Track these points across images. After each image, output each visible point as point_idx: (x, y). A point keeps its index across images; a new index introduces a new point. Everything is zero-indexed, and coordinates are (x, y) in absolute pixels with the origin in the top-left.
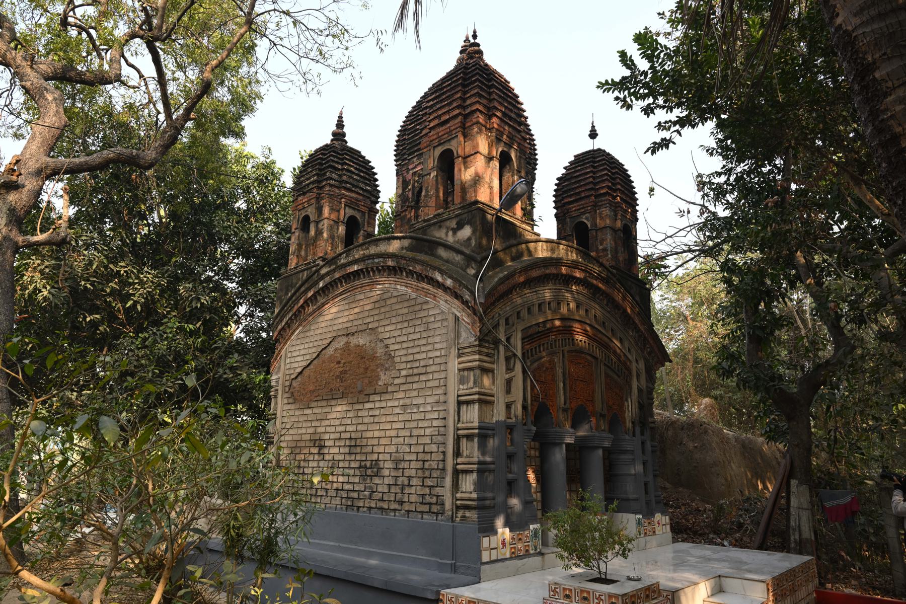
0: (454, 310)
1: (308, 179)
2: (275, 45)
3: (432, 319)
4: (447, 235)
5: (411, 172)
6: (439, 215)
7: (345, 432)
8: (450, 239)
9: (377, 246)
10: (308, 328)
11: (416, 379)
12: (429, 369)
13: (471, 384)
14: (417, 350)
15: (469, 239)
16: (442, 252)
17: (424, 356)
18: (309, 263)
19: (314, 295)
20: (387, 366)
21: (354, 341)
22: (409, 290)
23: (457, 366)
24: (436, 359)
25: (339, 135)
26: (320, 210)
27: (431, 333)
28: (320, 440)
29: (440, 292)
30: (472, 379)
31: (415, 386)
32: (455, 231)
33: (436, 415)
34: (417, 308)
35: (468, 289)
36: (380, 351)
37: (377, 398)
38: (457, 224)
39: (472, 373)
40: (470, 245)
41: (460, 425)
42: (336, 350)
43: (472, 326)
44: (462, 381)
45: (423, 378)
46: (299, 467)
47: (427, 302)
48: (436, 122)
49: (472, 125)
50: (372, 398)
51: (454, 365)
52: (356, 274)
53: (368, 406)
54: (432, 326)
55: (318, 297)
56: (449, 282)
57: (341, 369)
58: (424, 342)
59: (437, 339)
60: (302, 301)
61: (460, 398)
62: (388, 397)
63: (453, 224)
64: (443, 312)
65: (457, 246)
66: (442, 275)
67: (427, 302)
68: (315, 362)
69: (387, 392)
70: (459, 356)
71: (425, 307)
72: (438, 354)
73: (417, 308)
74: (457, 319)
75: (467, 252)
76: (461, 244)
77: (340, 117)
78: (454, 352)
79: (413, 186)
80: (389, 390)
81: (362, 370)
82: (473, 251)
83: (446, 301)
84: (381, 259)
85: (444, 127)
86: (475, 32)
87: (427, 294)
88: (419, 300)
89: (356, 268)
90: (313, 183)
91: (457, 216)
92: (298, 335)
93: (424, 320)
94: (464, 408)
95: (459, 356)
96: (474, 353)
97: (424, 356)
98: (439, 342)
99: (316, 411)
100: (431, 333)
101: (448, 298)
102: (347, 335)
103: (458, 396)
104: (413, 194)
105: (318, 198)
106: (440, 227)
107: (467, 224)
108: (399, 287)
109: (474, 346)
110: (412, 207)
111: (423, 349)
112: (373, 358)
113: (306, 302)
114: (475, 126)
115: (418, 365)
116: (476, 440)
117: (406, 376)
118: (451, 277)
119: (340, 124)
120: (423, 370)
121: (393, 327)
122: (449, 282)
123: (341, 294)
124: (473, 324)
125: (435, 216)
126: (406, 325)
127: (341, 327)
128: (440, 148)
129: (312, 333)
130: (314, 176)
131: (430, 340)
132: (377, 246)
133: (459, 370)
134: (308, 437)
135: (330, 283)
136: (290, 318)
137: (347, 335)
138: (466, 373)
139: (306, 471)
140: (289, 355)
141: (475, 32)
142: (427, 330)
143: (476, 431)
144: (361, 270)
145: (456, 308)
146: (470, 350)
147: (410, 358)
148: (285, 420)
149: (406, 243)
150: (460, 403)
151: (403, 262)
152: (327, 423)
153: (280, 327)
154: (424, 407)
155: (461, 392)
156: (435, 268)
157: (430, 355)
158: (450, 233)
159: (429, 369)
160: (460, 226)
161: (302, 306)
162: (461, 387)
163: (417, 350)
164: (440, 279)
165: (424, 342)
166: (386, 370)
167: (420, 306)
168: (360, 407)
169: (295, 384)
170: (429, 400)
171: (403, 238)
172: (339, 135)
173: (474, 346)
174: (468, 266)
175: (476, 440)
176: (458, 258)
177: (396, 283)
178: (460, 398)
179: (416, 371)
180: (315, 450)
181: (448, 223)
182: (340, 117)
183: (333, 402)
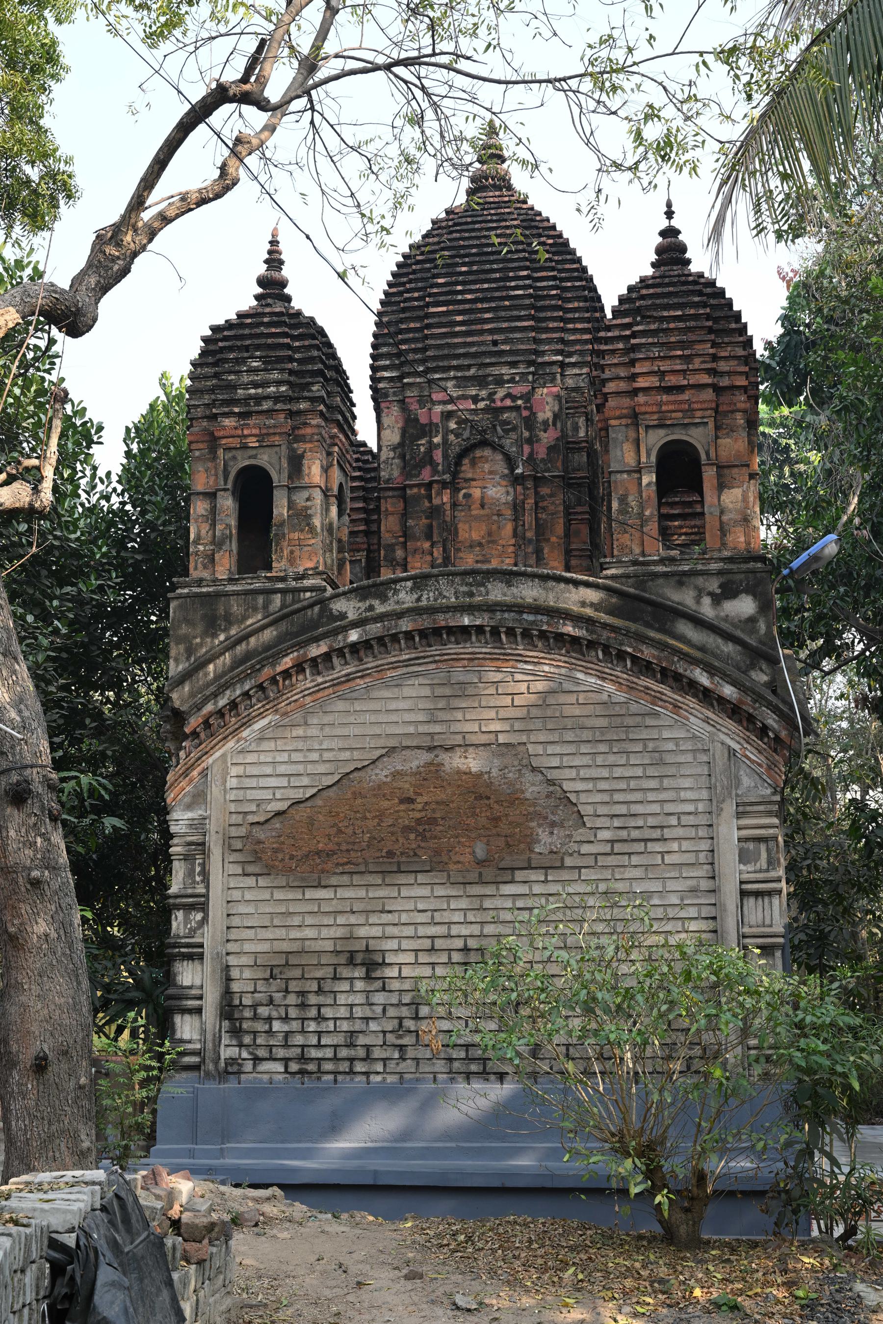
0: (723, 737)
1: (256, 385)
2: (312, 109)
3: (671, 746)
4: (698, 602)
5: (438, 409)
6: (672, 560)
7: (449, 936)
8: (707, 609)
9: (509, 584)
10: (297, 717)
11: (640, 847)
12: (668, 833)
13: (763, 863)
14: (638, 796)
15: (752, 620)
16: (685, 628)
17: (656, 808)
18: (283, 579)
19: (327, 657)
20: (556, 818)
21: (456, 762)
22: (610, 687)
23: (736, 834)
24: (683, 817)
25: (272, 286)
26: (296, 464)
27: (671, 771)
28: (367, 950)
29: (691, 702)
30: (764, 855)
31: (635, 860)
32: (717, 600)
33: (693, 912)
34: (629, 721)
35: (776, 710)
36: (532, 787)
37: (535, 875)
38: (720, 587)
39: (763, 847)
40: (754, 631)
41: (746, 930)
42: (396, 774)
43: (769, 767)
44: (744, 857)
45: (652, 847)
46: (303, 1006)
47: (656, 715)
48: (654, 381)
49: (733, 412)
50: (519, 875)
51: (729, 832)
52: (465, 630)
53: (507, 889)
54: (669, 758)
55: (335, 660)
56: (728, 691)
57: (418, 815)
58: (653, 784)
59: (687, 783)
60: (287, 662)
61: (744, 886)
62: (565, 875)
63: (714, 585)
64: (695, 737)
65: (724, 626)
66: (712, 675)
67: (656, 715)
68: (331, 793)
69: (562, 867)
70: (739, 815)
71: (649, 721)
72: (690, 808)
73: (629, 721)
74: (731, 753)
75: (752, 641)
76: (733, 625)
77: (274, 243)
78: (730, 808)
79: (445, 440)
80: (568, 862)
81: (483, 821)
82: (761, 642)
83: (706, 720)
84: (545, 618)
85: (672, 398)
86: (669, 205)
87: (656, 699)
88: (634, 708)
89: (466, 621)
90: (277, 398)
91: (720, 573)
92: (262, 730)
93: (651, 745)
94: (751, 902)
95: (739, 815)
96: (769, 814)
97: (656, 808)
98: (689, 791)
99: (342, 893)
100: (671, 771)
101: (710, 714)
102: (430, 749)
103: (741, 883)
104: (445, 456)
105: (293, 436)
106: (681, 584)
107: (747, 591)
108: (580, 676)
109: (771, 803)
110: (444, 485)
111: (651, 796)
112: (514, 799)
113: (299, 667)
114: (739, 416)
115: (640, 823)
116: (778, 954)
117: (612, 842)
118: (734, 683)
119: (274, 261)
120: (656, 834)
121: (570, 749)
122: (728, 691)
123: (407, 663)
124: (771, 766)
125: (662, 561)
126: (603, 748)
127: (411, 729)
128: (662, 432)
129: (313, 731)
130: (279, 383)
131: (666, 782)
132: (509, 584)
133: (739, 840)
134: (329, 946)
135: (380, 640)
136: (246, 695)
137: (430, 749)
138: (751, 846)
139: (327, 1012)
140: (234, 771)
141: (669, 205)
142: (661, 763)
143: (781, 940)
145: (729, 735)
146: (761, 808)
147: (622, 809)
149: (593, 596)
150: (743, 894)
151: (605, 634)
152: (386, 918)
153: (209, 707)
154: (661, 898)
155: (745, 877)
156: (695, 662)
157: (669, 808)
158: (707, 601)
159: (668, 833)
160: (729, 592)
161: (286, 674)
162: (742, 867)
163: (638, 796)
164: (704, 680)
165: (653, 784)
166: (553, 824)
167: (638, 719)
168: (489, 890)
169: (260, 833)
170: (672, 885)
171: (587, 585)
172: (272, 286)
173: (771, 803)
174: (752, 666)
175: (778, 954)
176: (729, 648)
177: (572, 667)
178: (744, 886)
179: (635, 834)
180: (359, 972)
181: (700, 581)
182: (274, 243)
183: (402, 879)
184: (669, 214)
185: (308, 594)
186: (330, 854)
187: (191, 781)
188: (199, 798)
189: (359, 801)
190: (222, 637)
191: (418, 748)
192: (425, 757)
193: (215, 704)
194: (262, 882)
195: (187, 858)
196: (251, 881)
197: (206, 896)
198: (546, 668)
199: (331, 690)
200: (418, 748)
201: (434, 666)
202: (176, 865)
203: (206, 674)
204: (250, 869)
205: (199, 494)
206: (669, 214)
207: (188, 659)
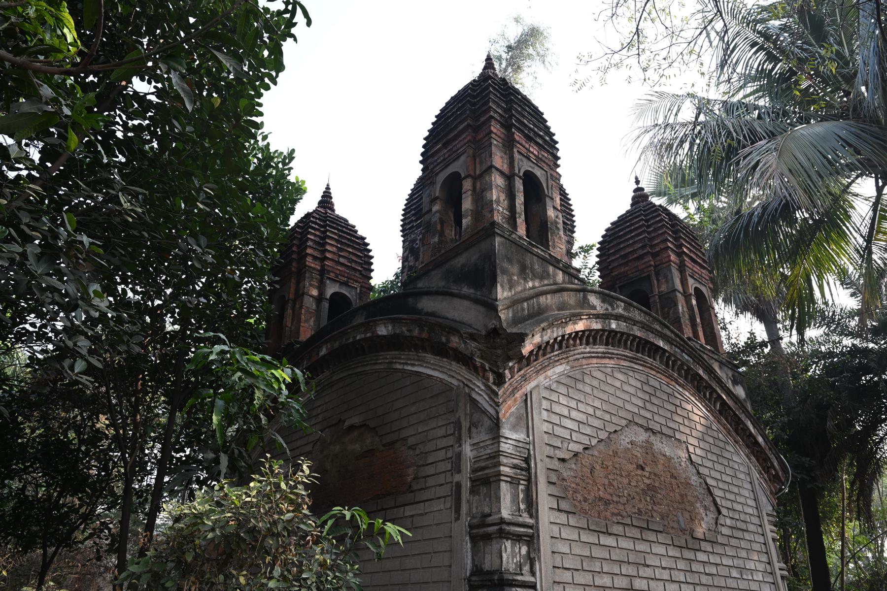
1: (534, 125)
81: (678, 497)
89: (661, 344)
102: (647, 429)
141: (636, 178)
144: (665, 351)
148: (563, 548)
152: (648, 572)
184: (637, 182)
185: (576, 281)
186: (607, 503)
187: (515, 400)
188: (525, 420)
189: (617, 459)
190: (530, 284)
191: (642, 426)
192: (642, 436)
193: (542, 337)
194: (573, 521)
195: (514, 482)
196: (562, 518)
197: (535, 527)
198: (687, 394)
199: (595, 361)
200: (642, 426)
201: (641, 368)
202: (503, 485)
203: (523, 309)
204: (564, 505)
205: (497, 169)
206: (637, 182)
207: (510, 289)
